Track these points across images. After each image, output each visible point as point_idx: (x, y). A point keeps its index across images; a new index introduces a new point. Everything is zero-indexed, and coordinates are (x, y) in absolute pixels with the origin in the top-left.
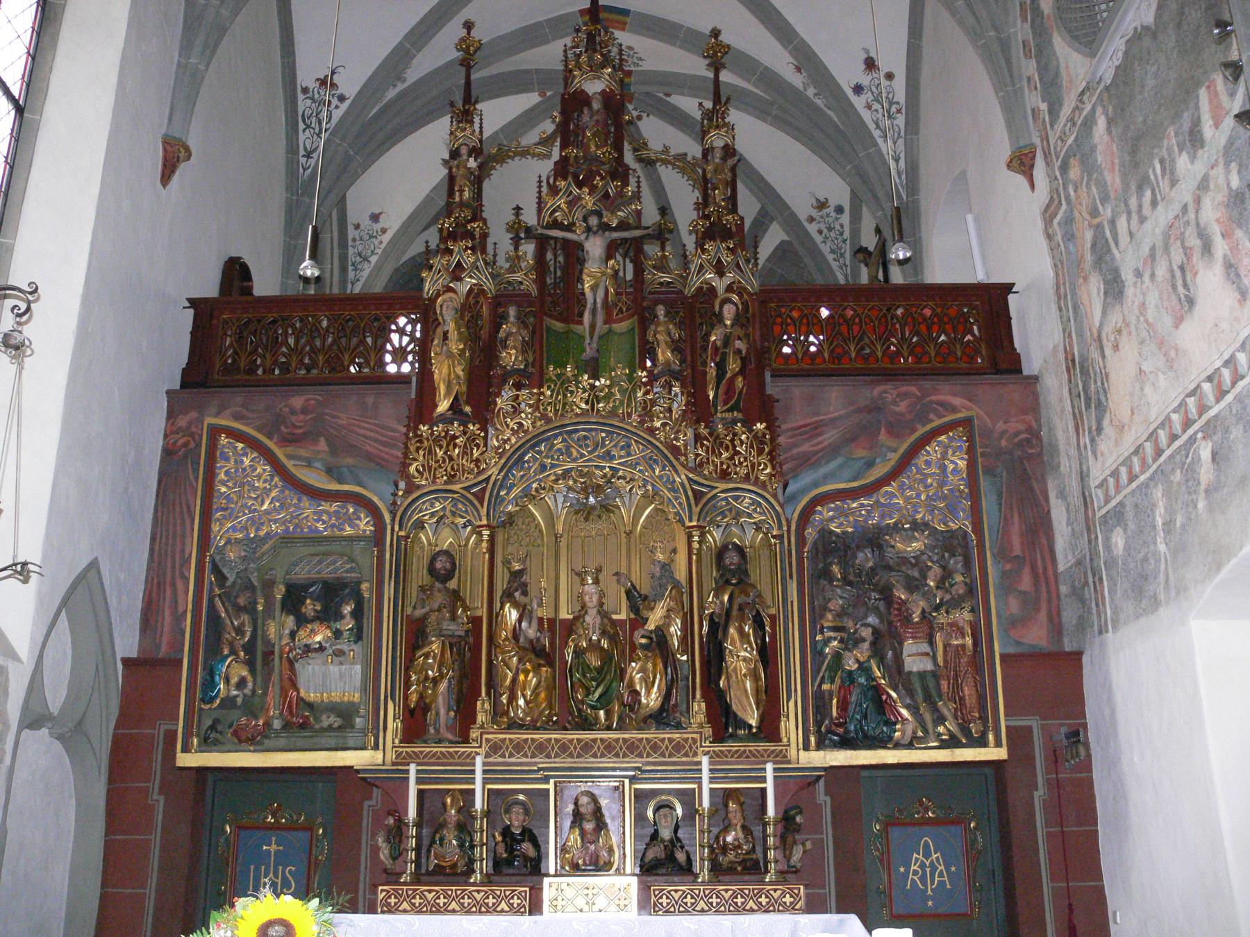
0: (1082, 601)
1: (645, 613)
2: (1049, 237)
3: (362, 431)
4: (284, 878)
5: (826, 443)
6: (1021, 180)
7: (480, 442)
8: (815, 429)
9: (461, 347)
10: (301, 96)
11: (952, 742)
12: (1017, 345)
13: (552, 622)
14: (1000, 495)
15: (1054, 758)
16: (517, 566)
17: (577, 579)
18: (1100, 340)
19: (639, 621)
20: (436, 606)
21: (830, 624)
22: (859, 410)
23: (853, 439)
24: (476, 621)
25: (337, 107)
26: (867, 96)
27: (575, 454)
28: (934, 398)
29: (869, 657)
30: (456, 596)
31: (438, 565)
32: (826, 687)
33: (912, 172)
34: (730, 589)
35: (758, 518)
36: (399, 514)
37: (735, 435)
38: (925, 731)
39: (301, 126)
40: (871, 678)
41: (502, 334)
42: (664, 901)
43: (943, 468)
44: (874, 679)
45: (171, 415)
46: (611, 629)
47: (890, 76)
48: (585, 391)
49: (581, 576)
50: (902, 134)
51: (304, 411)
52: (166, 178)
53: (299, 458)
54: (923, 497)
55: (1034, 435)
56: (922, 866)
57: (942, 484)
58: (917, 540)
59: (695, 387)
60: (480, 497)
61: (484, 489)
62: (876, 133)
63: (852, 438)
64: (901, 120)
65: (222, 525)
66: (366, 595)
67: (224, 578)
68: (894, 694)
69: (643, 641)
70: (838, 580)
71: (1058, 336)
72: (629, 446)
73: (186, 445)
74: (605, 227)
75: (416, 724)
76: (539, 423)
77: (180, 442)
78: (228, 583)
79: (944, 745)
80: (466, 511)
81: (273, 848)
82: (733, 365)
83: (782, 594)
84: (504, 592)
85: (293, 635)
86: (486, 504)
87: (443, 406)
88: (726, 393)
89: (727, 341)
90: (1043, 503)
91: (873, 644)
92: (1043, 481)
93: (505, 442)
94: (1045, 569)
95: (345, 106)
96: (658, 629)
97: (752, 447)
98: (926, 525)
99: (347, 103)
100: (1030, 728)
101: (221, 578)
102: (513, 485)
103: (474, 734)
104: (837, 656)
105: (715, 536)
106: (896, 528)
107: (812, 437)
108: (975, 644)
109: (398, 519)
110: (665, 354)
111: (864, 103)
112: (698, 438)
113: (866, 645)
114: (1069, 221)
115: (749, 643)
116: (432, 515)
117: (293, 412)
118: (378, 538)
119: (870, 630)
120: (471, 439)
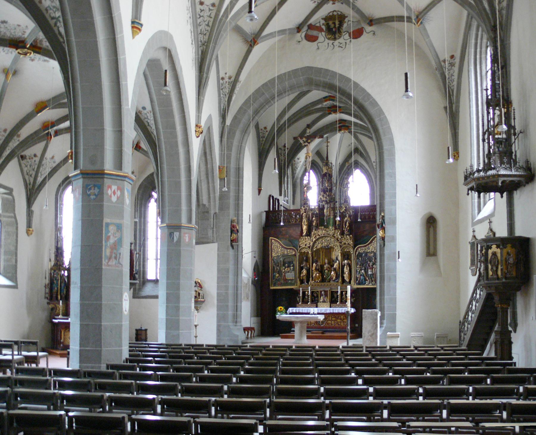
52: (259, 194)
75: (302, 282)
87: (304, 234)
101: (274, 262)
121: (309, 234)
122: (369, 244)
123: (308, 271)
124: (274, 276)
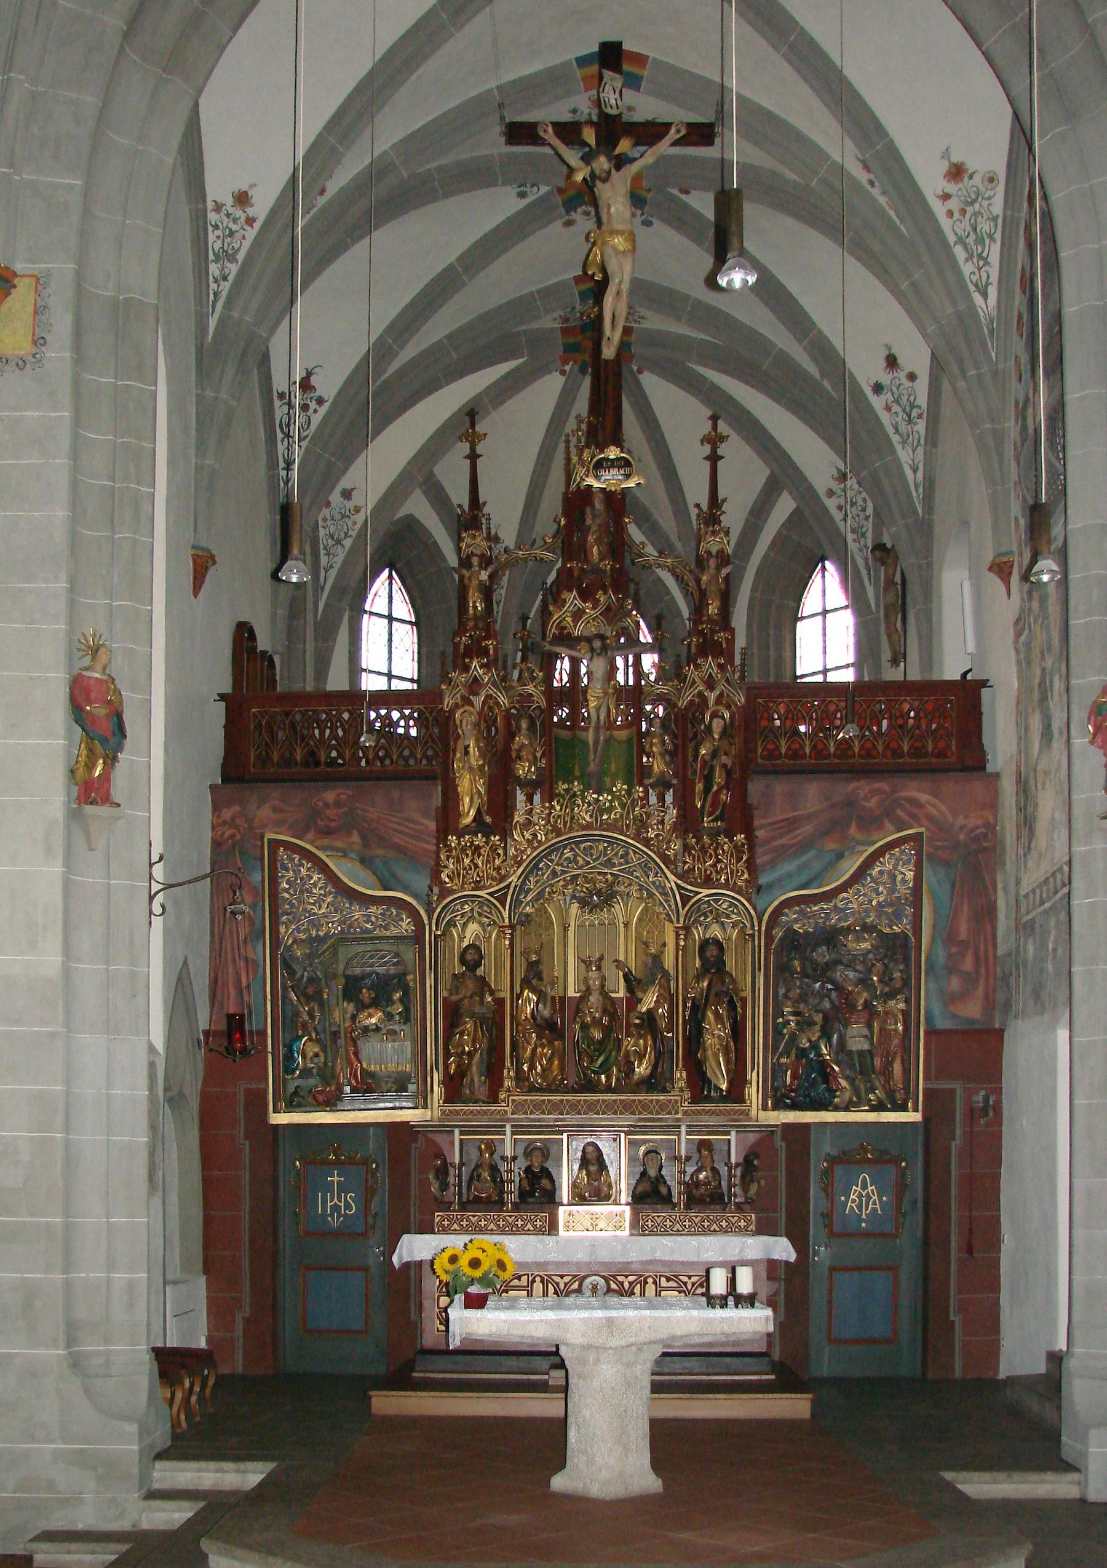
0: (1008, 987)
1: (640, 995)
3: (390, 825)
5: (799, 838)
7: (501, 851)
8: (792, 824)
9: (481, 762)
10: (277, 403)
11: (879, 1107)
12: (985, 741)
13: (562, 999)
14: (953, 886)
15: (972, 1114)
16: (534, 958)
17: (583, 965)
18: (1035, 771)
19: (633, 1001)
20: (469, 994)
21: (789, 1009)
22: (833, 806)
23: (826, 834)
24: (500, 1002)
25: (315, 411)
26: (886, 397)
27: (581, 862)
28: (903, 794)
29: (819, 1038)
30: (483, 982)
31: (469, 957)
32: (784, 1060)
33: (930, 484)
34: (708, 976)
35: (735, 918)
36: (435, 916)
37: (718, 844)
38: (859, 1097)
39: (280, 435)
40: (819, 1054)
41: (515, 746)
42: (650, 1223)
43: (893, 877)
44: (822, 1055)
45: (216, 808)
46: (610, 1006)
47: (912, 377)
48: (589, 804)
49: (587, 964)
50: (922, 442)
51: (338, 804)
53: (333, 849)
54: (874, 903)
55: (990, 828)
56: (860, 1196)
57: (892, 891)
58: (865, 940)
59: (684, 801)
60: (502, 900)
61: (506, 894)
62: (895, 439)
63: (826, 833)
64: (921, 426)
65: (287, 928)
66: (411, 984)
67: (295, 973)
68: (836, 1068)
69: (637, 1021)
70: (798, 973)
71: (1014, 748)
72: (627, 854)
73: (233, 836)
76: (550, 836)
77: (227, 834)
78: (298, 976)
79: (874, 1109)
80: (490, 913)
82: (719, 778)
83: (753, 983)
84: (522, 980)
85: (354, 1018)
86: (507, 907)
88: (712, 805)
89: (714, 754)
90: (991, 892)
91: (823, 1027)
92: (993, 873)
93: (523, 852)
94: (986, 952)
95: (323, 410)
96: (649, 1010)
97: (732, 856)
98: (875, 927)
99: (326, 406)
100: (952, 1091)
101: (292, 972)
102: (530, 890)
103: (502, 1096)
104: (793, 1037)
105: (698, 933)
106: (848, 930)
107: (789, 832)
108: (906, 1028)
109: (434, 921)
110: (658, 766)
111: (884, 406)
112: (686, 848)
113: (818, 1027)
115: (723, 1024)
116: (463, 915)
117: (327, 805)
118: (418, 938)
119: (821, 1015)
120: (494, 849)
121: (497, 818)
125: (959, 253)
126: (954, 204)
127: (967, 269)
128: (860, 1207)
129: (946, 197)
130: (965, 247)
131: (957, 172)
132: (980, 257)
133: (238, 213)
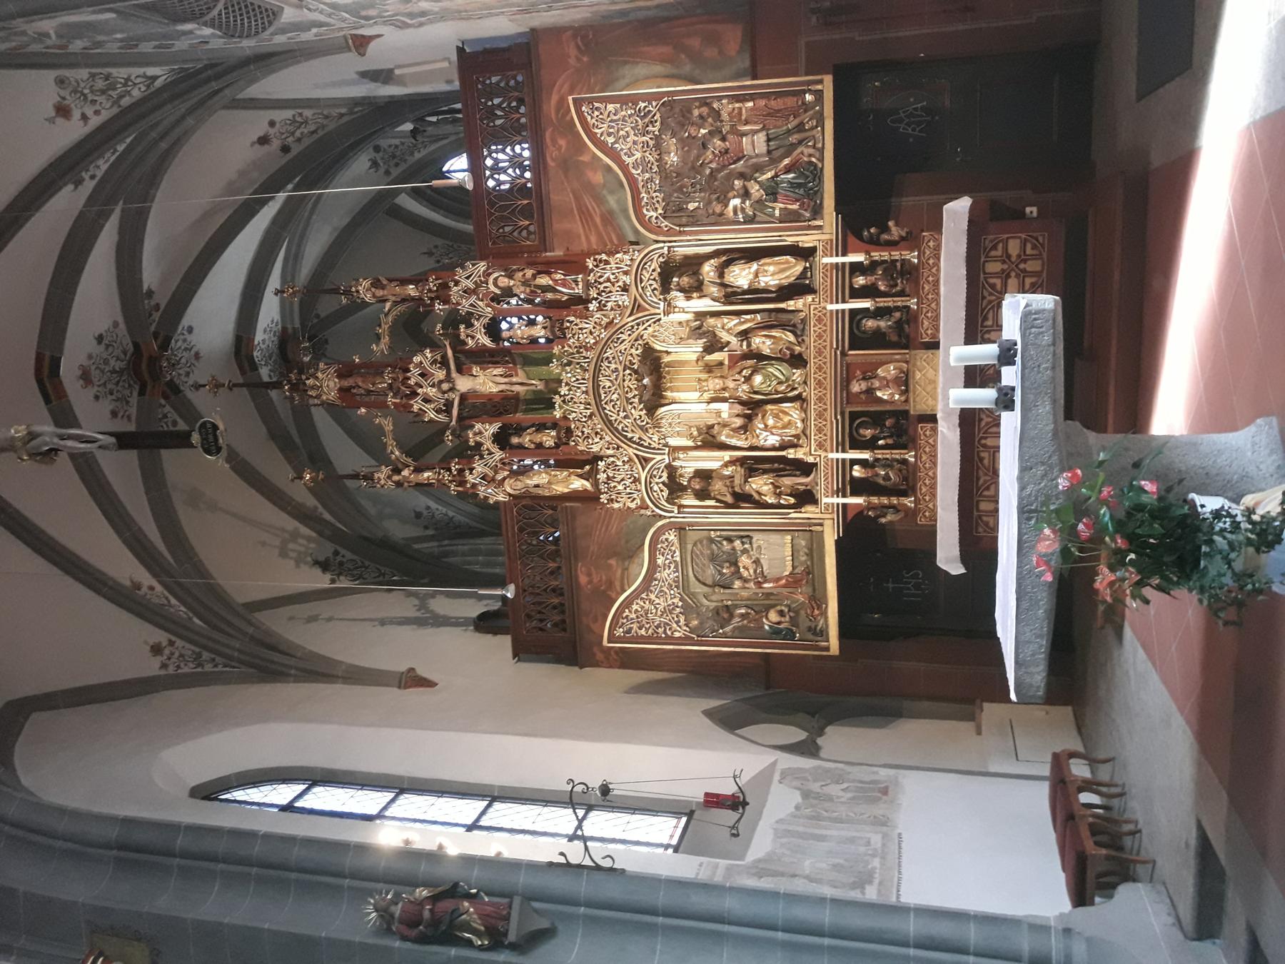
2: (421, 25)
4: (912, 577)
6: (373, 45)
51: (589, 575)
56: (908, 124)
60: (647, 460)
74: (448, 378)
75: (806, 498)
81: (891, 585)
82: (544, 280)
100: (807, 44)
103: (811, 460)
107: (590, 215)
114: (411, 15)
122: (624, 167)
123: (752, 466)
124: (776, 632)
125: (126, 101)
126: (89, 111)
127: (136, 93)
128: (919, 124)
129: (84, 118)
130: (121, 97)
131: (63, 111)
132: (125, 85)
133: (167, 652)
